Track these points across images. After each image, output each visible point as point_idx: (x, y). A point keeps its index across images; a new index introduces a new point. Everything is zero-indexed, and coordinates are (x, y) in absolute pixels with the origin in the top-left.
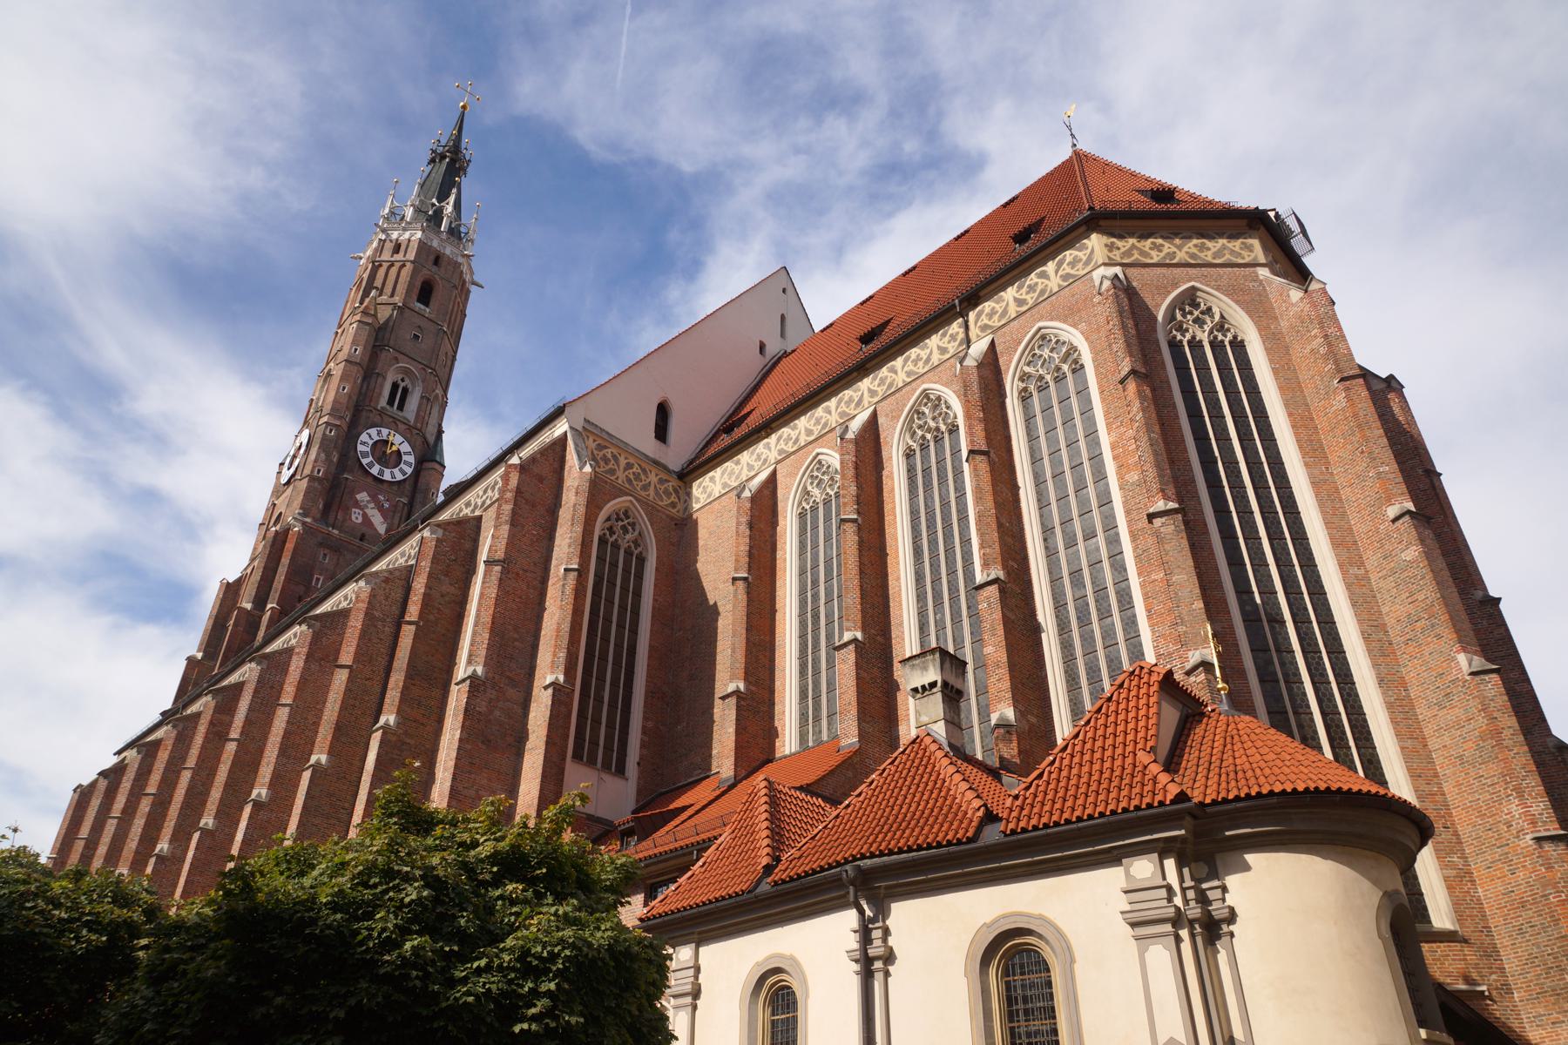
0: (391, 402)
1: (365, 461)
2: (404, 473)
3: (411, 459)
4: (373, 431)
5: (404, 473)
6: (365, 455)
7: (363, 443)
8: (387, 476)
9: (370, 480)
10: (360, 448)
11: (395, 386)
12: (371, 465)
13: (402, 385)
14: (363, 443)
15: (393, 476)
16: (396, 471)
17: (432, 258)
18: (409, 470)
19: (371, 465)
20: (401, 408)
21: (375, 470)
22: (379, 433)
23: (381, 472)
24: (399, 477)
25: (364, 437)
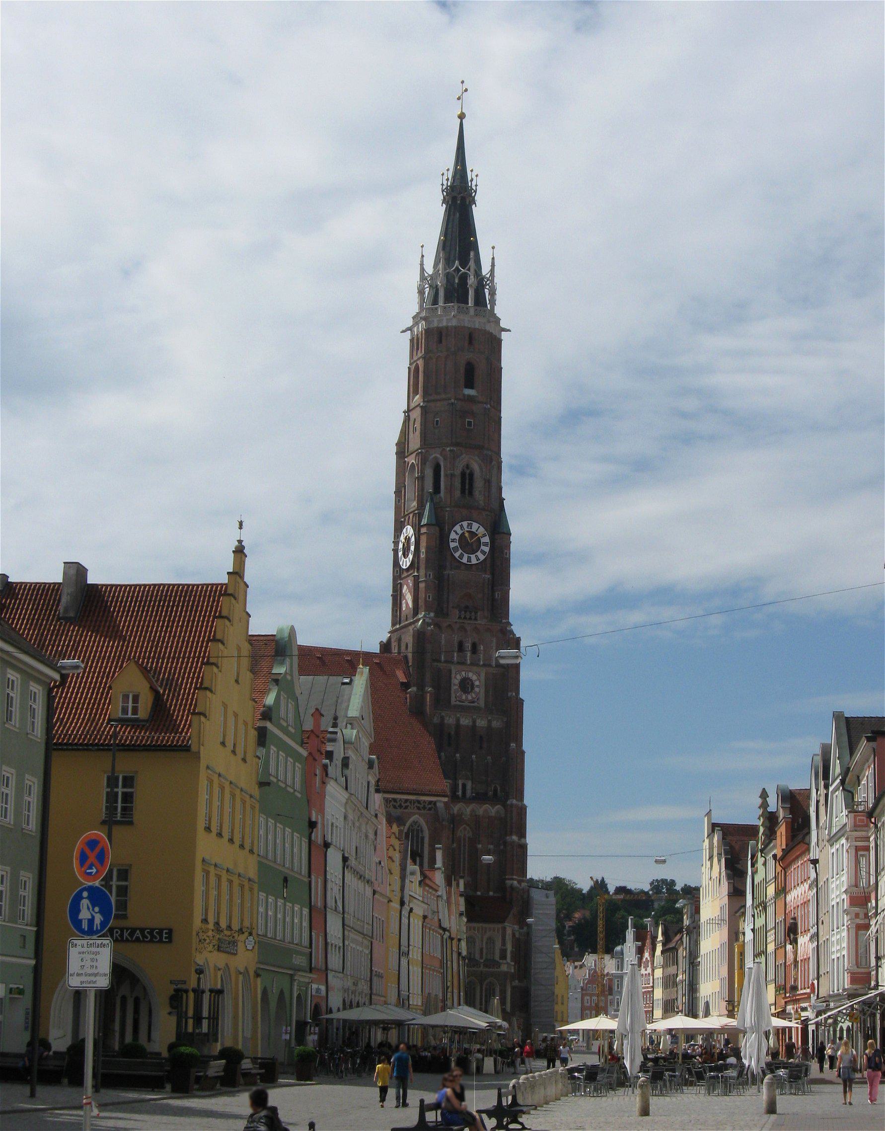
0: (463, 491)
1: (457, 555)
2: (483, 552)
3: (486, 539)
4: (457, 528)
5: (483, 552)
7: (453, 540)
9: (463, 567)
10: (452, 545)
11: (463, 474)
12: (461, 556)
14: (453, 540)
15: (478, 559)
16: (479, 554)
17: (467, 338)
21: (465, 560)
22: (462, 526)
23: (469, 559)
25: (453, 535)
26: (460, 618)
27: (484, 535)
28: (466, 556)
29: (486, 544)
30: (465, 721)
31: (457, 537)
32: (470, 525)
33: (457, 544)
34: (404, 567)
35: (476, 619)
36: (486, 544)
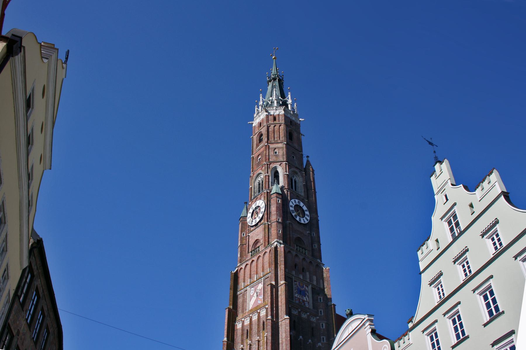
1: (293, 214)
8: (302, 222)
14: (291, 206)
16: (304, 218)
19: (296, 216)
21: (298, 219)
24: (307, 222)
25: (291, 204)
29: (307, 215)
30: (304, 316)
33: (293, 209)
34: (254, 224)
35: (305, 253)
36: (307, 215)
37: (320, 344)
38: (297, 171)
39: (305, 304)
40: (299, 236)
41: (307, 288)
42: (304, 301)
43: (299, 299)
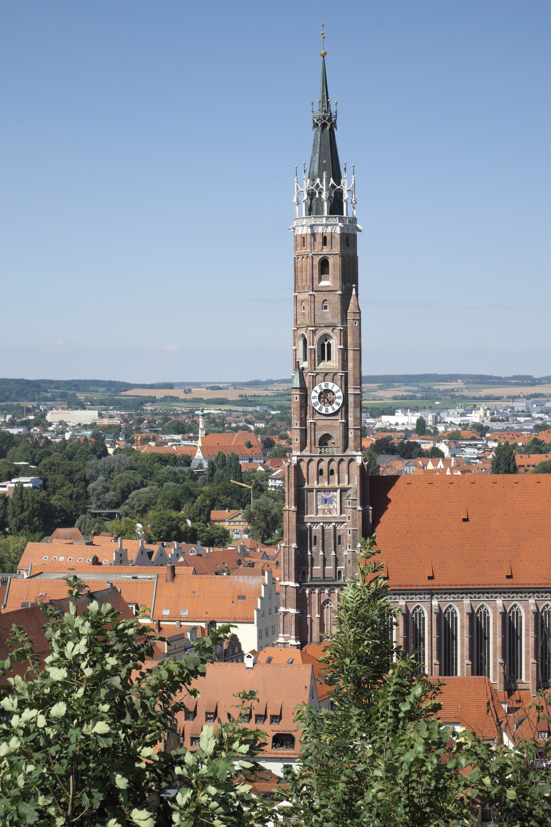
1: (317, 408)
2: (338, 404)
3: (340, 394)
6: (316, 404)
7: (314, 398)
13: (326, 343)
14: (314, 398)
16: (334, 405)
18: (340, 401)
19: (321, 409)
20: (329, 358)
21: (323, 411)
22: (320, 386)
23: (327, 410)
24: (337, 408)
25: (314, 394)
26: (321, 453)
27: (338, 391)
28: (324, 408)
29: (339, 398)
31: (317, 395)
32: (326, 385)
33: (317, 400)
36: (339, 398)
37: (345, 553)
38: (328, 331)
39: (331, 513)
40: (325, 432)
41: (335, 493)
42: (330, 511)
43: (324, 510)
